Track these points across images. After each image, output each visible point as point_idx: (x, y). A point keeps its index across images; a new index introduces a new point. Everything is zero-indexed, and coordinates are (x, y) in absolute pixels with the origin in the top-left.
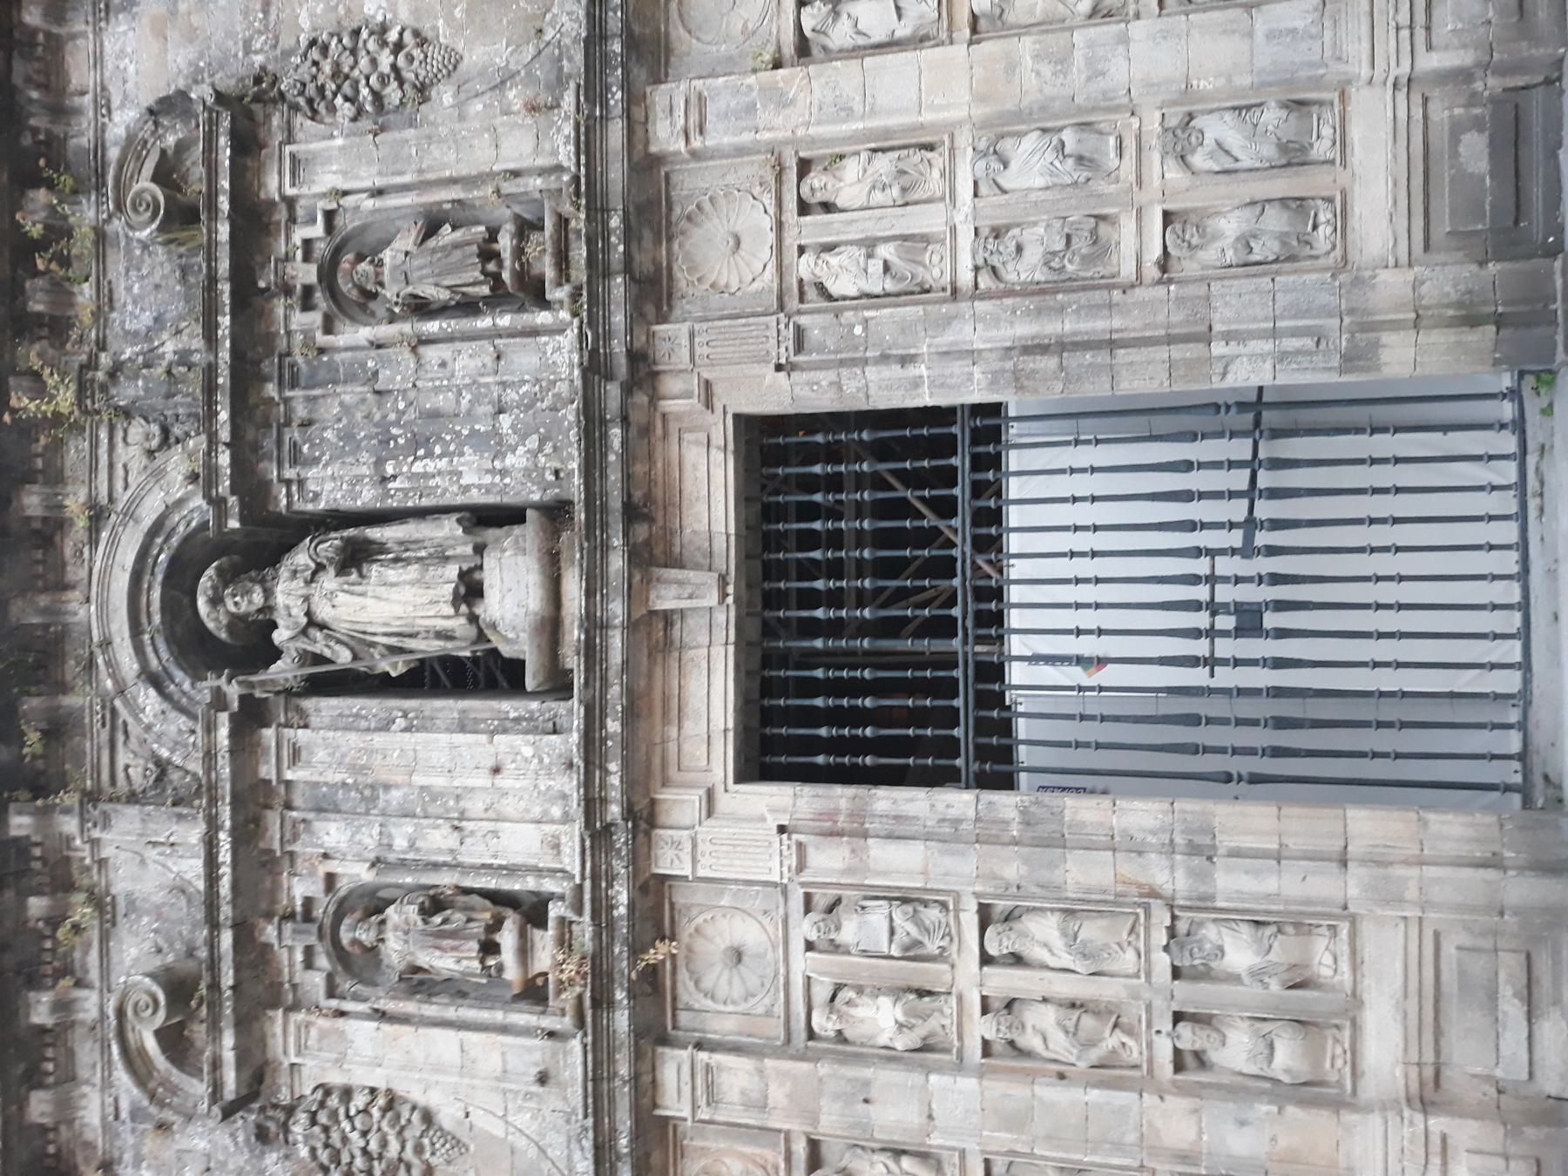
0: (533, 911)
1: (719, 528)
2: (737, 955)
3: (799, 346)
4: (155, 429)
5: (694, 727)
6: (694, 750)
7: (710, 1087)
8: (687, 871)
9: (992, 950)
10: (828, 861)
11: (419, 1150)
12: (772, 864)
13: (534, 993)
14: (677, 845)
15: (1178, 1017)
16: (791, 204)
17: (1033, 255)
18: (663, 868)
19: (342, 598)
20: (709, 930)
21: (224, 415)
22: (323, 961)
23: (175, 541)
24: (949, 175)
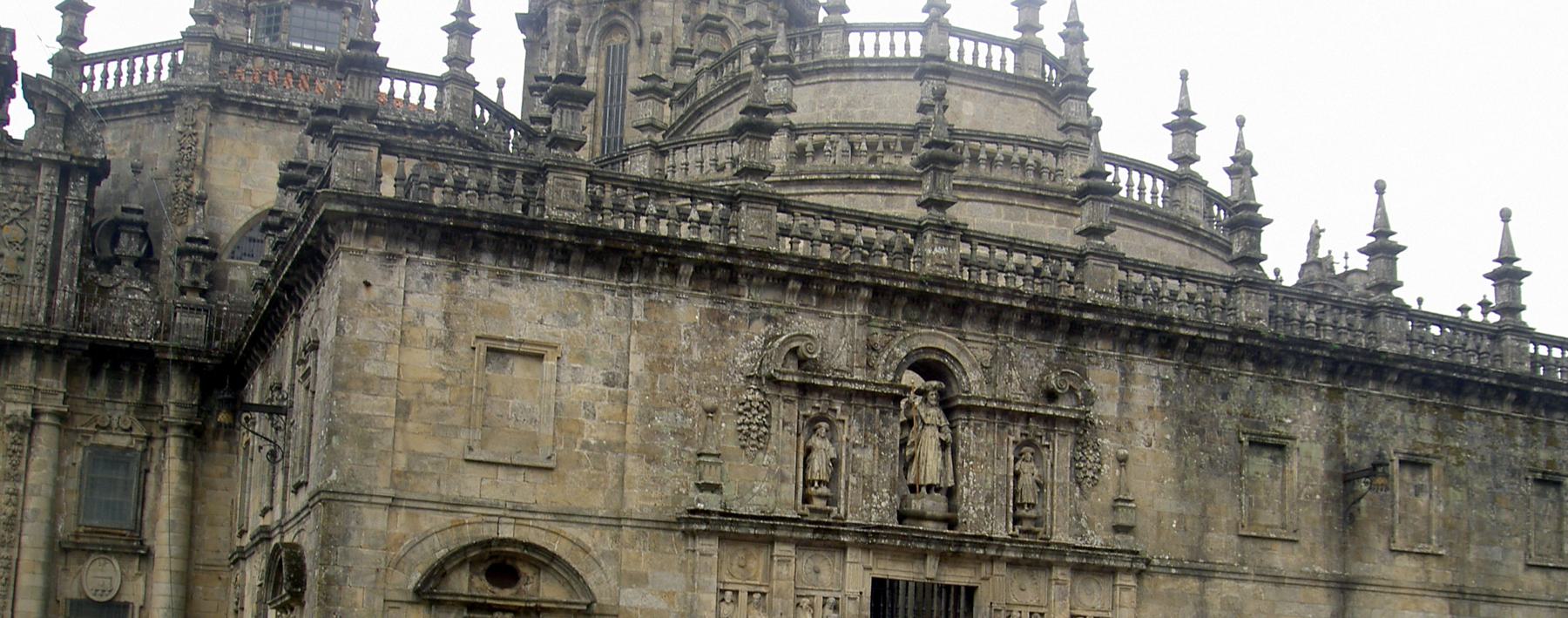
0: (831, 500)
1: (947, 579)
2: (817, 572)
4: (988, 365)
5: (889, 565)
6: (882, 564)
7: (784, 561)
8: (849, 559)
11: (753, 446)
12: (851, 589)
13: (807, 499)
14: (856, 557)
16: (1033, 610)
18: (849, 551)
19: (934, 440)
20: (826, 563)
21: (995, 404)
22: (814, 413)
23: (951, 367)
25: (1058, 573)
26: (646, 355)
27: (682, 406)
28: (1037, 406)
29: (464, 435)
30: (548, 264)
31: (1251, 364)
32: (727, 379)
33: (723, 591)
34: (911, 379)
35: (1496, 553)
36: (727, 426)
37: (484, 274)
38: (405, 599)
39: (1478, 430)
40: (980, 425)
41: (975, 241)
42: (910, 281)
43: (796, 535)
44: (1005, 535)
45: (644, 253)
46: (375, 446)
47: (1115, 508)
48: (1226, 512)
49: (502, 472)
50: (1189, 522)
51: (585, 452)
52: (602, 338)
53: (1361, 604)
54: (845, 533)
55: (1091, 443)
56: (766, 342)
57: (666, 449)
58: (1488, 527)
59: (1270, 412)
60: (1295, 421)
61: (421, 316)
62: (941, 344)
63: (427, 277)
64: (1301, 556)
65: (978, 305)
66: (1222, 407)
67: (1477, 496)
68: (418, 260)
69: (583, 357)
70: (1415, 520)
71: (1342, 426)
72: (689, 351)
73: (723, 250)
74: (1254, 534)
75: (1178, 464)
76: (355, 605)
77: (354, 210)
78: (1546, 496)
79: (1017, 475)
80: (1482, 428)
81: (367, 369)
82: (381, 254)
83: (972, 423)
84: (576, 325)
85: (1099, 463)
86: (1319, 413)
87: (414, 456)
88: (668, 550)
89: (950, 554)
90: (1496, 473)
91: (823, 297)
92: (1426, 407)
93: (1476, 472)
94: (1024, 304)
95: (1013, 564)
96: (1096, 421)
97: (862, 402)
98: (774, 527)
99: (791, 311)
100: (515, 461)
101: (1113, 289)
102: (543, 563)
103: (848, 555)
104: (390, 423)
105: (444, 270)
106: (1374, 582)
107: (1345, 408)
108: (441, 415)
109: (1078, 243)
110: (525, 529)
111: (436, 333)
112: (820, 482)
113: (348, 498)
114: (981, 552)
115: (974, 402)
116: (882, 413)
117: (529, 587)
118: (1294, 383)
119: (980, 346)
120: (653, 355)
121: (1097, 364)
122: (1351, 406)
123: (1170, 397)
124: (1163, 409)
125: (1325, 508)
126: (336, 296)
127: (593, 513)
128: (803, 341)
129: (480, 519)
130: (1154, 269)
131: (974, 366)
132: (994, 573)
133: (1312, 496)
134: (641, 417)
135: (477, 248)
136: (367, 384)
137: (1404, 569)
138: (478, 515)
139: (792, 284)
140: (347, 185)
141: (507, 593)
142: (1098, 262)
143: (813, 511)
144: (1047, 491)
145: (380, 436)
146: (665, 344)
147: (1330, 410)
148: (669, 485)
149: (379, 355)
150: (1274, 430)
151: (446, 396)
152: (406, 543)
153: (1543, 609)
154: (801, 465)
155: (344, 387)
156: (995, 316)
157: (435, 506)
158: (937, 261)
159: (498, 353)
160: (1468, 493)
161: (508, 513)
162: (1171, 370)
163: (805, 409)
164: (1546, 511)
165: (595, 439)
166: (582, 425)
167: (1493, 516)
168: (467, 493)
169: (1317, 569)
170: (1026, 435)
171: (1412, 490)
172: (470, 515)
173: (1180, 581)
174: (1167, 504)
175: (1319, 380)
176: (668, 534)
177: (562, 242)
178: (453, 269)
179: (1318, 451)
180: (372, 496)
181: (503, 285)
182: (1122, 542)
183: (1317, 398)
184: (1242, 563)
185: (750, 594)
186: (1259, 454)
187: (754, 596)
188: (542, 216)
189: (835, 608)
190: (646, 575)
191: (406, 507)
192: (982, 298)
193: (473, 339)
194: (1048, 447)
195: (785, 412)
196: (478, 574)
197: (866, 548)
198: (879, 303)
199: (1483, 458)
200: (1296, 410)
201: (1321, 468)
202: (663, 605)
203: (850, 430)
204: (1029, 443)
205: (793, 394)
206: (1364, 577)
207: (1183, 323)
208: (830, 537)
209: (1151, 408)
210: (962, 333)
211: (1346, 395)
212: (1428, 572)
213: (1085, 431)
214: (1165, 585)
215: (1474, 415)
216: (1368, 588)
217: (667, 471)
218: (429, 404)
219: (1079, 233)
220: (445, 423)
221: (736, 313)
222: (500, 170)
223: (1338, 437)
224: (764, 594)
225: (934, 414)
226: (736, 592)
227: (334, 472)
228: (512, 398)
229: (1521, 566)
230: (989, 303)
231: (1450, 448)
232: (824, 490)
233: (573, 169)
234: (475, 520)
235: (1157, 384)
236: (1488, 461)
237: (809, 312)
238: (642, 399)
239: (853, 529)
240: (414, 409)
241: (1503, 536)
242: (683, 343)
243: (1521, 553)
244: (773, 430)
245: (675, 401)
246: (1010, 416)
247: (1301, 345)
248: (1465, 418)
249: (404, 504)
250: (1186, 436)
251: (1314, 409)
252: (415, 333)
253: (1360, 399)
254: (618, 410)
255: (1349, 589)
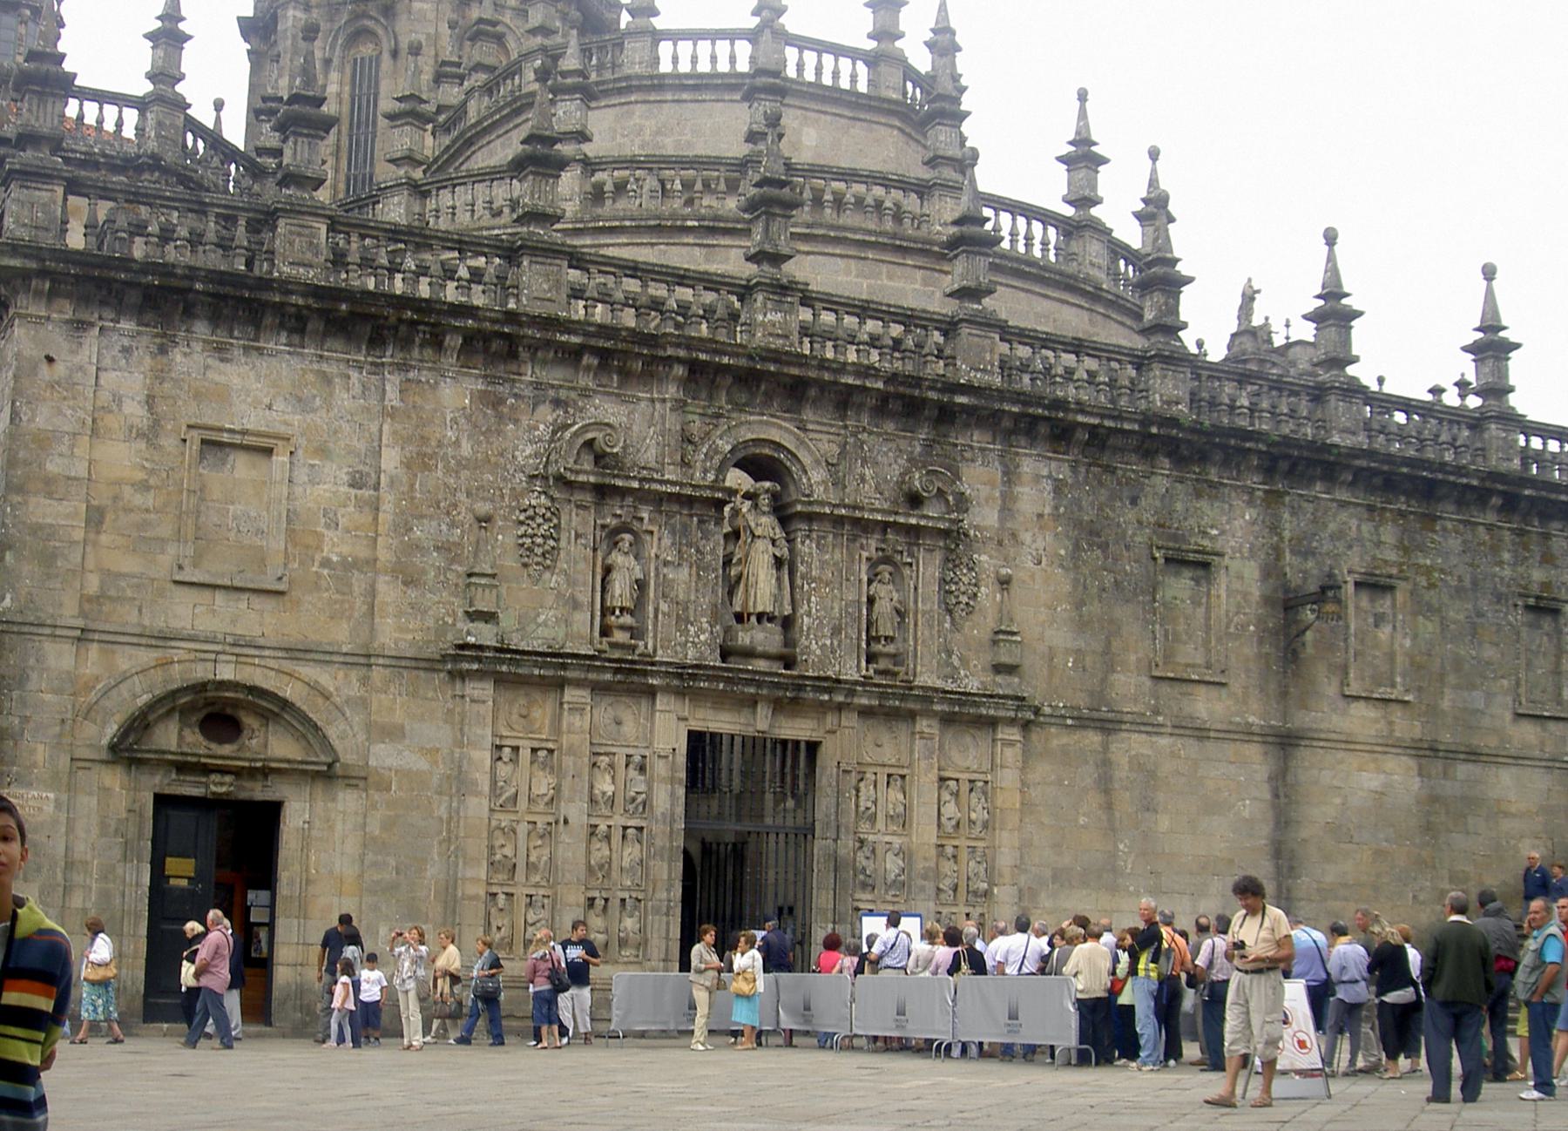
0: (636, 632)
2: (619, 723)
3: (845, 771)
4: (835, 461)
6: (700, 714)
7: (576, 709)
8: (658, 707)
9: (629, 831)
10: (660, 768)
11: (538, 564)
13: (605, 631)
14: (668, 704)
15: (606, 900)
16: (892, 771)
17: (865, 863)
18: (659, 697)
19: (766, 557)
20: (630, 711)
23: (788, 464)
24: (894, 834)
25: (923, 725)
26: (402, 449)
27: (448, 513)
28: (896, 513)
29: (172, 550)
30: (278, 334)
31: (1167, 461)
32: (504, 479)
33: (499, 748)
34: (737, 479)
35: (1477, 699)
36: (505, 539)
37: (197, 347)
38: (97, 758)
39: (1454, 543)
40: (824, 538)
41: (818, 305)
42: (737, 355)
43: (592, 676)
44: (856, 677)
45: (400, 320)
46: (59, 564)
47: (995, 643)
48: (1136, 647)
49: (220, 597)
50: (1088, 660)
51: (325, 572)
52: (346, 427)
53: (1307, 764)
54: (653, 674)
55: (965, 560)
56: (554, 433)
57: (427, 567)
58: (1467, 666)
59: (1192, 521)
60: (1222, 533)
61: (118, 399)
62: (775, 435)
63: (126, 351)
64: (1230, 703)
65: (822, 386)
66: (1130, 515)
68: (114, 329)
69: (323, 452)
70: (1375, 657)
71: (1282, 539)
72: (457, 444)
73: (499, 316)
74: (1171, 675)
75: (1075, 587)
76: (34, 765)
77: (33, 265)
78: (1540, 627)
79: (871, 601)
80: (1459, 541)
81: (51, 467)
82: (67, 322)
83: (814, 535)
84: (314, 411)
85: (975, 585)
86: (1253, 522)
87: (109, 576)
88: (430, 694)
89: (786, 701)
90: (1477, 599)
91: (626, 375)
92: (1388, 514)
93: (1451, 597)
94: (880, 385)
95: (866, 713)
96: (972, 532)
97: (675, 508)
98: (564, 666)
99: (585, 393)
100: (237, 583)
101: (993, 365)
102: (271, 711)
103: (658, 702)
104: (79, 535)
105: (146, 342)
106: (1323, 736)
107: (1286, 516)
108: (144, 525)
109: (949, 308)
110: (249, 669)
111: (137, 421)
112: (622, 609)
113: (26, 629)
114: (826, 697)
115: (817, 509)
116: (701, 522)
117: (254, 742)
118: (1221, 484)
119: (825, 437)
120: (411, 449)
121: (973, 461)
122: (1293, 514)
123: (1064, 502)
124: (1056, 517)
125: (1261, 642)
126: (10, 374)
127: (336, 649)
128: (601, 430)
129: (192, 656)
130: (1045, 340)
131: (817, 462)
132: (843, 723)
133: (1244, 627)
134: (396, 526)
135: (189, 313)
136: (50, 486)
137: (1361, 720)
138: (190, 650)
139: (587, 360)
140: (25, 234)
141: (227, 749)
142: (974, 332)
143: (614, 645)
144: (910, 620)
145: (66, 552)
146: (426, 434)
147: (1267, 519)
148: (430, 613)
149: (64, 449)
150: (1196, 544)
151: (150, 500)
152: (98, 687)
153: (1537, 770)
154: (598, 588)
155: (20, 490)
156: (844, 400)
157: (135, 640)
158: (771, 330)
159: (214, 446)
160: (1442, 624)
161: (227, 648)
162: (1066, 467)
163: (604, 518)
164: (1540, 646)
165: (338, 554)
166: (320, 536)
167: (1474, 653)
168: (176, 624)
169: (1251, 719)
170: (883, 550)
171: (1371, 620)
172: (180, 651)
173: (1077, 735)
174: (1061, 637)
175: (1254, 480)
176: (429, 675)
177: (296, 305)
178: (158, 340)
179: (1251, 571)
180: (55, 626)
181: (222, 360)
182: (1005, 686)
183: (1250, 503)
184: (1156, 712)
185: (534, 750)
186: (1177, 574)
187: (539, 753)
188: (271, 272)
189: (642, 769)
190: (403, 727)
191: (100, 641)
192: (827, 376)
193: (184, 428)
194: (911, 564)
195: (578, 521)
196: (190, 726)
197: (680, 693)
198: (697, 383)
199: (1460, 579)
200: (1225, 518)
201: (1256, 592)
202: (422, 764)
203: (660, 544)
204: (887, 560)
205: (588, 498)
206: (1310, 729)
207: (1081, 408)
208: (635, 679)
209: (1040, 516)
210: (801, 421)
211: (1287, 499)
212: (1391, 723)
213: (958, 545)
214: (1058, 739)
215: (1449, 525)
216: (1315, 743)
217: (429, 595)
218: (128, 510)
219: (951, 295)
220: (148, 534)
221: (516, 396)
222: (217, 215)
223: (1277, 551)
224: (551, 751)
225: (766, 524)
226: (516, 749)
227: (8, 596)
228: (233, 503)
229: (1508, 716)
230: (835, 383)
231: (1419, 566)
232: (627, 619)
233: (310, 214)
234: (186, 657)
235: (1048, 486)
236: (1467, 583)
237: (609, 394)
238: (397, 505)
239: (663, 669)
240: (109, 517)
241: (1485, 678)
242: (449, 434)
243: (1509, 699)
244: (563, 544)
245: (439, 507)
246: (862, 526)
247: (1230, 436)
248: (1438, 528)
249: (96, 637)
250: (1086, 552)
251: (1247, 517)
252: (111, 421)
253: (1305, 505)
254: (366, 518)
255: (1291, 745)
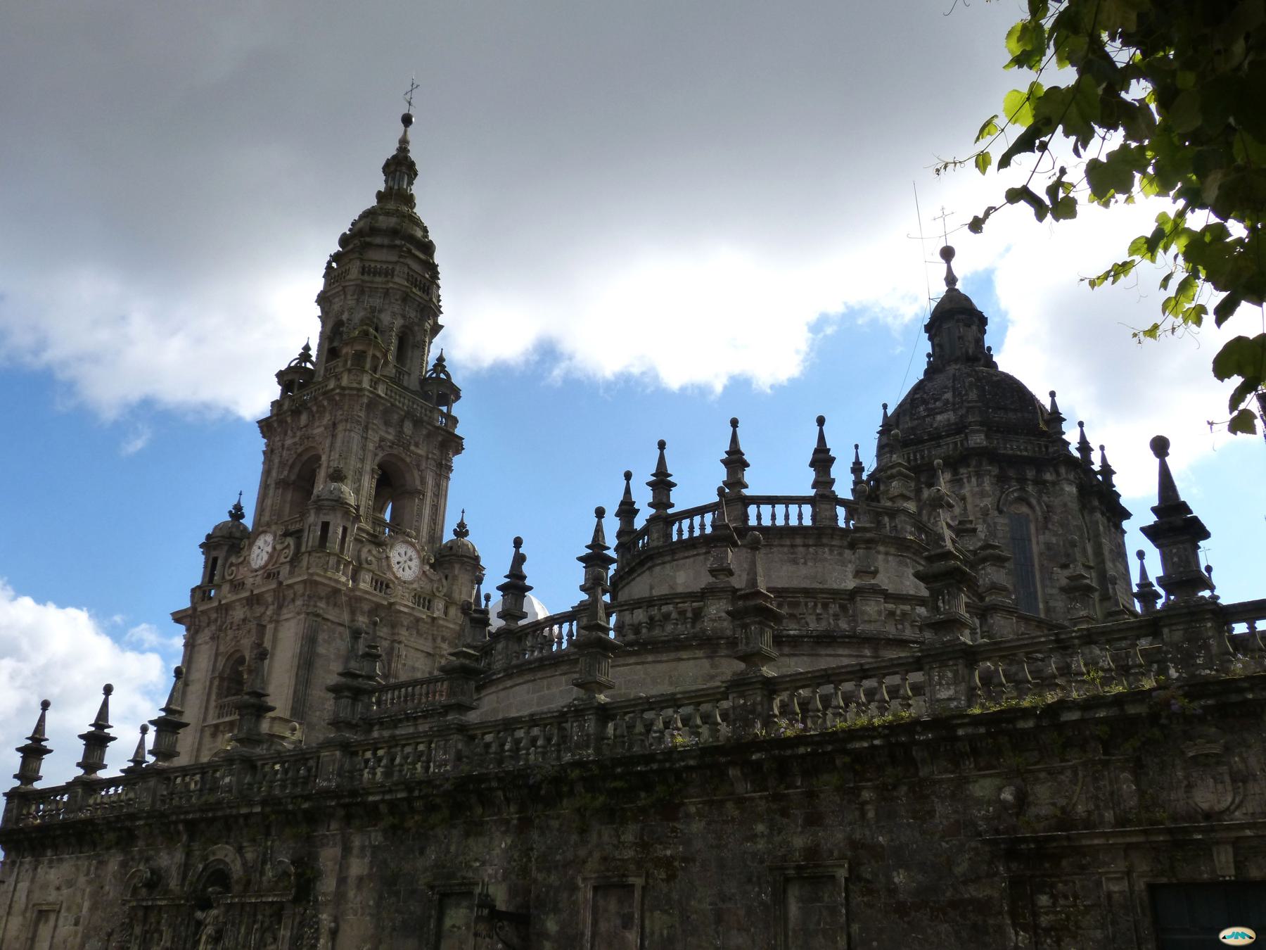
60: (483, 863)
67: (694, 916)
80: (703, 824)
107: (536, 837)
215: (693, 809)
223: (525, 871)
251: (503, 846)
